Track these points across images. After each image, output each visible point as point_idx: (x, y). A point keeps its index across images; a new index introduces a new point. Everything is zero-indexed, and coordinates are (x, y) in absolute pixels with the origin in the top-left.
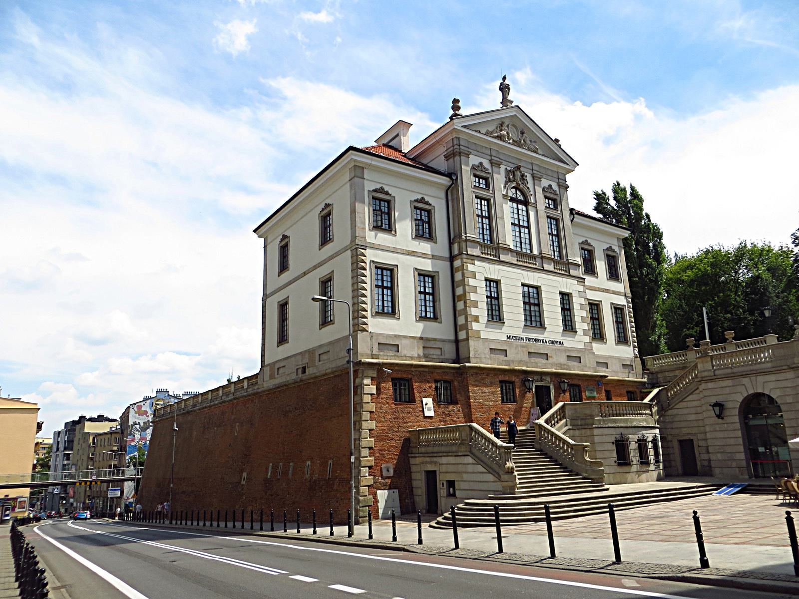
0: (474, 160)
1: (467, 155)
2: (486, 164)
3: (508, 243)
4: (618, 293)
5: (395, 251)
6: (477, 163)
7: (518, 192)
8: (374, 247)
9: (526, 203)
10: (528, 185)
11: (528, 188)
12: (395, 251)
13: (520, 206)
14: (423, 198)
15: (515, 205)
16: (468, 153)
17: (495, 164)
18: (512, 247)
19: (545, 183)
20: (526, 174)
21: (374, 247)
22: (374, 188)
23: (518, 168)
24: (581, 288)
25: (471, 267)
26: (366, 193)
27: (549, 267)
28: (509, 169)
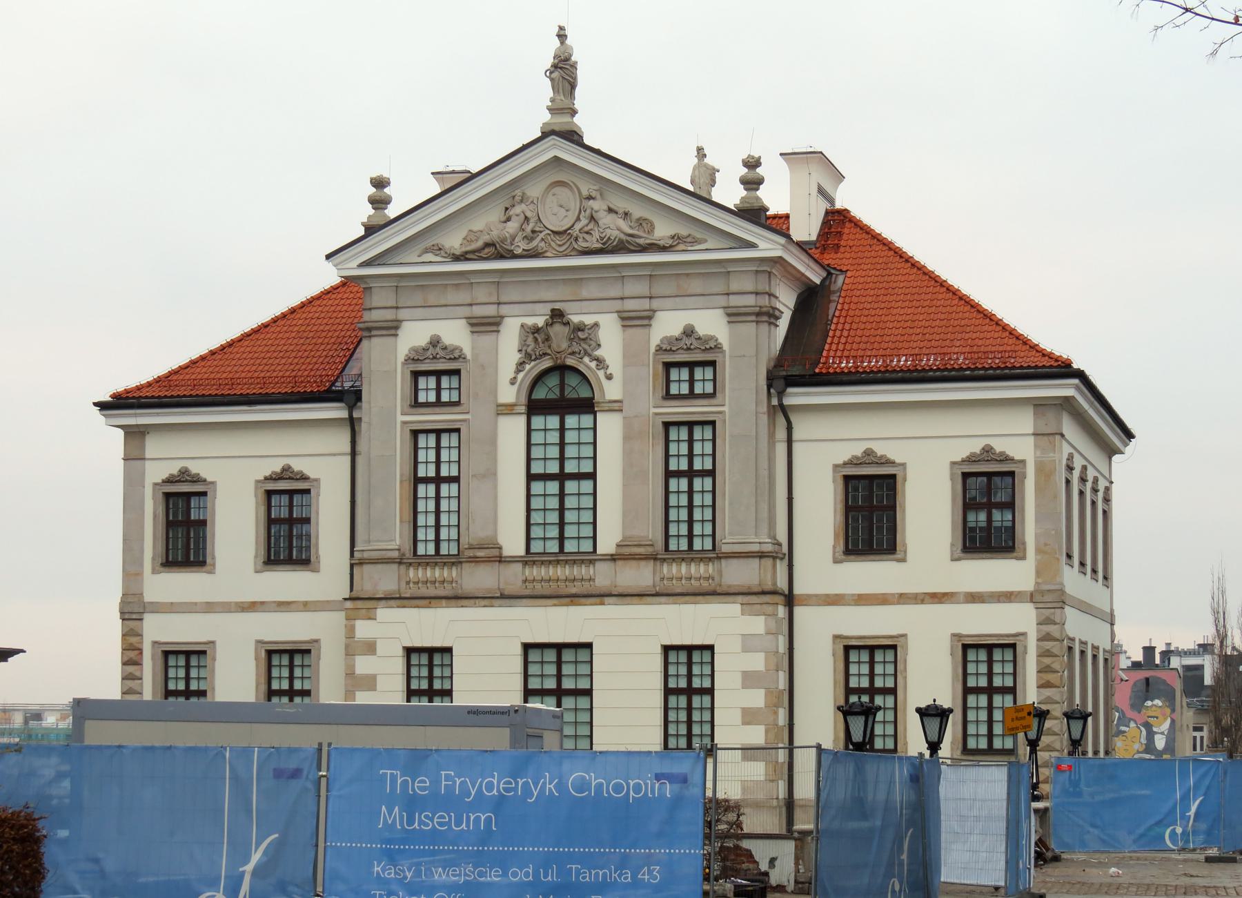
0: (414, 335)
1: (392, 328)
2: (454, 333)
3: (502, 540)
4: (1007, 597)
5: (209, 608)
6: (422, 341)
7: (572, 380)
8: (158, 608)
9: (587, 406)
10: (598, 353)
11: (600, 361)
12: (209, 608)
13: (571, 421)
14: (287, 469)
15: (553, 421)
16: (394, 324)
17: (486, 325)
18: (513, 544)
19: (668, 324)
20: (588, 320)
21: (158, 608)
22: (165, 476)
23: (557, 315)
24: (757, 625)
25: (363, 629)
26: (148, 491)
27: (640, 575)
28: (530, 321)
